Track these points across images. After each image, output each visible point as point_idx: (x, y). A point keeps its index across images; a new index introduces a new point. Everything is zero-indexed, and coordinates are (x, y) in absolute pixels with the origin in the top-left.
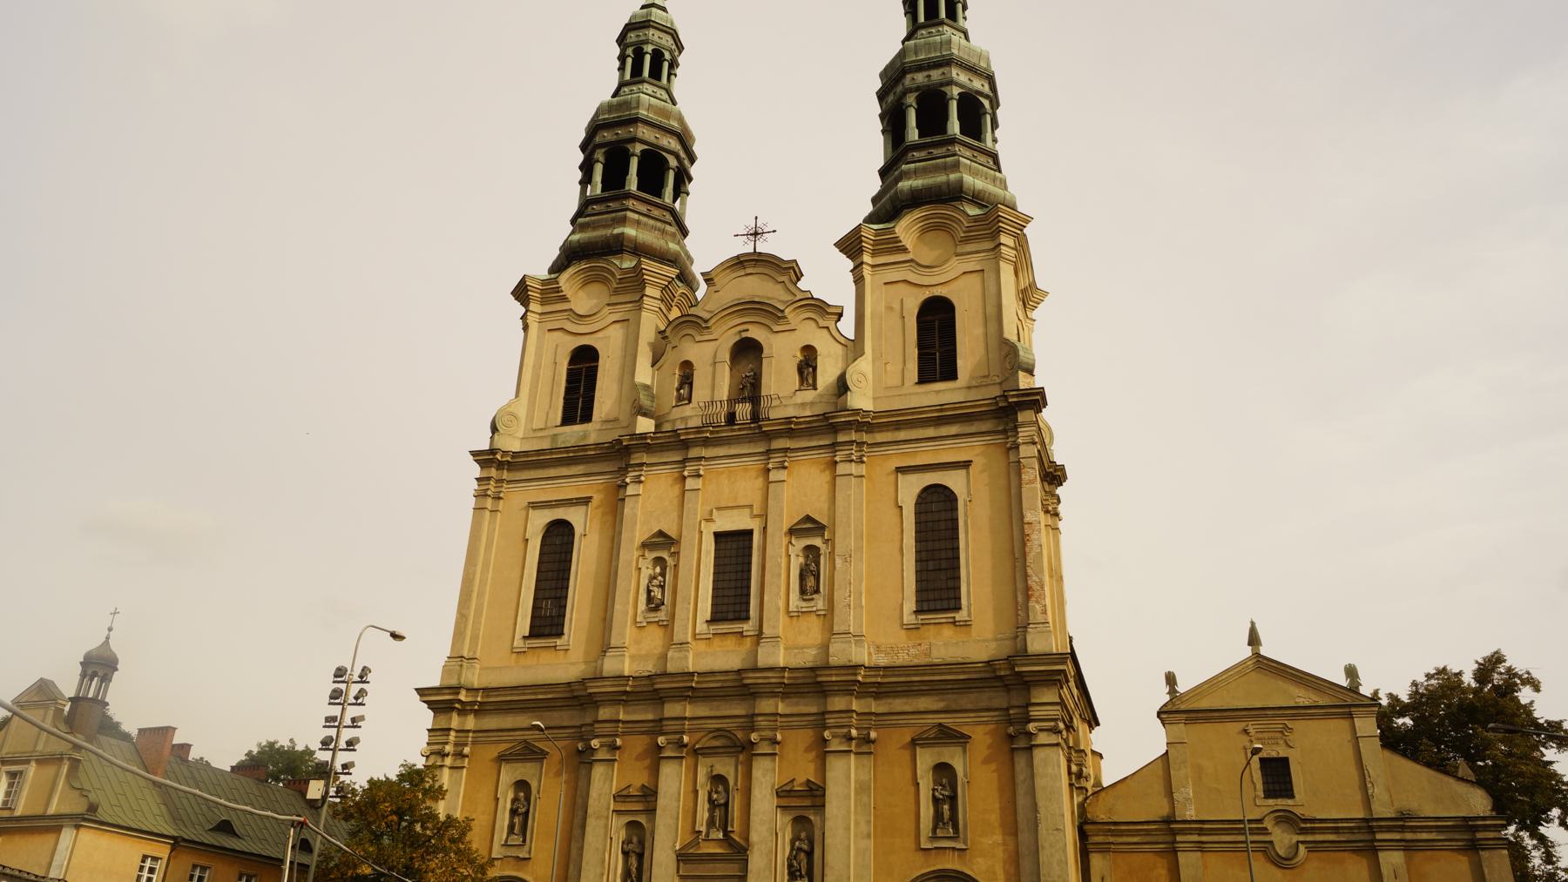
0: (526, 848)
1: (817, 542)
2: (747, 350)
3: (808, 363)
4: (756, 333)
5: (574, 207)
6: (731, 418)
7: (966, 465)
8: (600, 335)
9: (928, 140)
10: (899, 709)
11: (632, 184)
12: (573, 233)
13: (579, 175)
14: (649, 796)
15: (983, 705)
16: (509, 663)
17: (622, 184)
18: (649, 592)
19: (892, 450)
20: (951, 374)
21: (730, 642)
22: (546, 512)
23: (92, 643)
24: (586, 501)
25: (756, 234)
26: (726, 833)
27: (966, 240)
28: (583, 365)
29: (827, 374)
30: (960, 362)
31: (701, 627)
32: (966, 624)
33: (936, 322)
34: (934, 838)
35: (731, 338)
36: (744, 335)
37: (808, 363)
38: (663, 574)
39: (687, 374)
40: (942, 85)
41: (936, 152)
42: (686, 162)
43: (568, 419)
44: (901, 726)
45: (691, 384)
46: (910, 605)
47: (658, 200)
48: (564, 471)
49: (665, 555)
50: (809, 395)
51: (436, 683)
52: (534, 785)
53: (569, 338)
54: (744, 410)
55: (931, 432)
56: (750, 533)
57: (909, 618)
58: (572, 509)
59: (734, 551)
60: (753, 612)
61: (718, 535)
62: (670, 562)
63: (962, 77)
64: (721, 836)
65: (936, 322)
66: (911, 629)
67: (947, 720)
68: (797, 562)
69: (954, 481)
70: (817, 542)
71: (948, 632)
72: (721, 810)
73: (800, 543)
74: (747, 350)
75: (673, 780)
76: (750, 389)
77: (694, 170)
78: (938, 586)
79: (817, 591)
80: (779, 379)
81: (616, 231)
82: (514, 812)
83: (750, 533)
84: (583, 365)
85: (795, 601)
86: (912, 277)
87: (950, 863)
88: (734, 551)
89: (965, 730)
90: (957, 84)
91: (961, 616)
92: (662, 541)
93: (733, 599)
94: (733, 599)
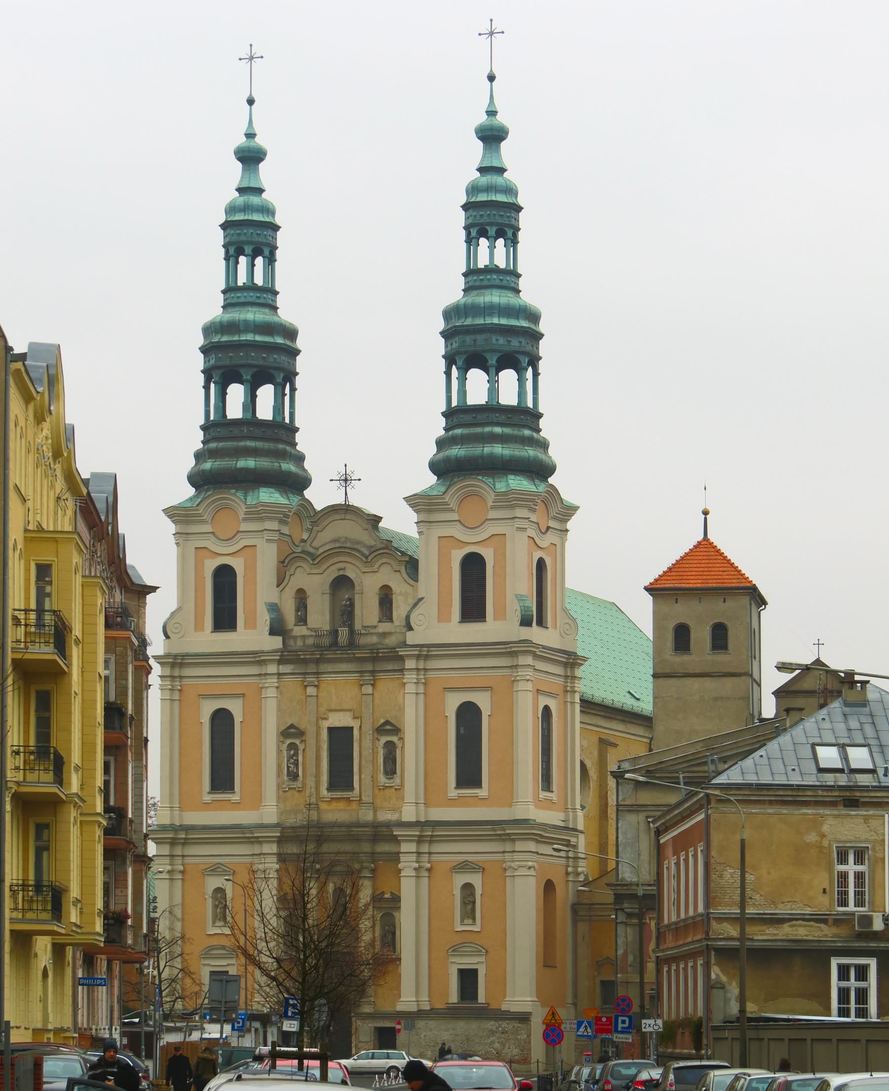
18: (288, 767)
21: (342, 805)
25: (346, 480)
28: (224, 579)
31: (324, 792)
35: (332, 574)
38: (296, 754)
39: (301, 598)
45: (306, 608)
49: (297, 742)
54: (343, 632)
59: (341, 740)
61: (330, 729)
62: (301, 747)
70: (394, 739)
74: (342, 583)
76: (345, 613)
79: (395, 773)
80: (367, 612)
82: (216, 907)
84: (224, 579)
85: (382, 779)
88: (341, 740)
90: (494, 351)
93: (341, 776)
94: (341, 776)
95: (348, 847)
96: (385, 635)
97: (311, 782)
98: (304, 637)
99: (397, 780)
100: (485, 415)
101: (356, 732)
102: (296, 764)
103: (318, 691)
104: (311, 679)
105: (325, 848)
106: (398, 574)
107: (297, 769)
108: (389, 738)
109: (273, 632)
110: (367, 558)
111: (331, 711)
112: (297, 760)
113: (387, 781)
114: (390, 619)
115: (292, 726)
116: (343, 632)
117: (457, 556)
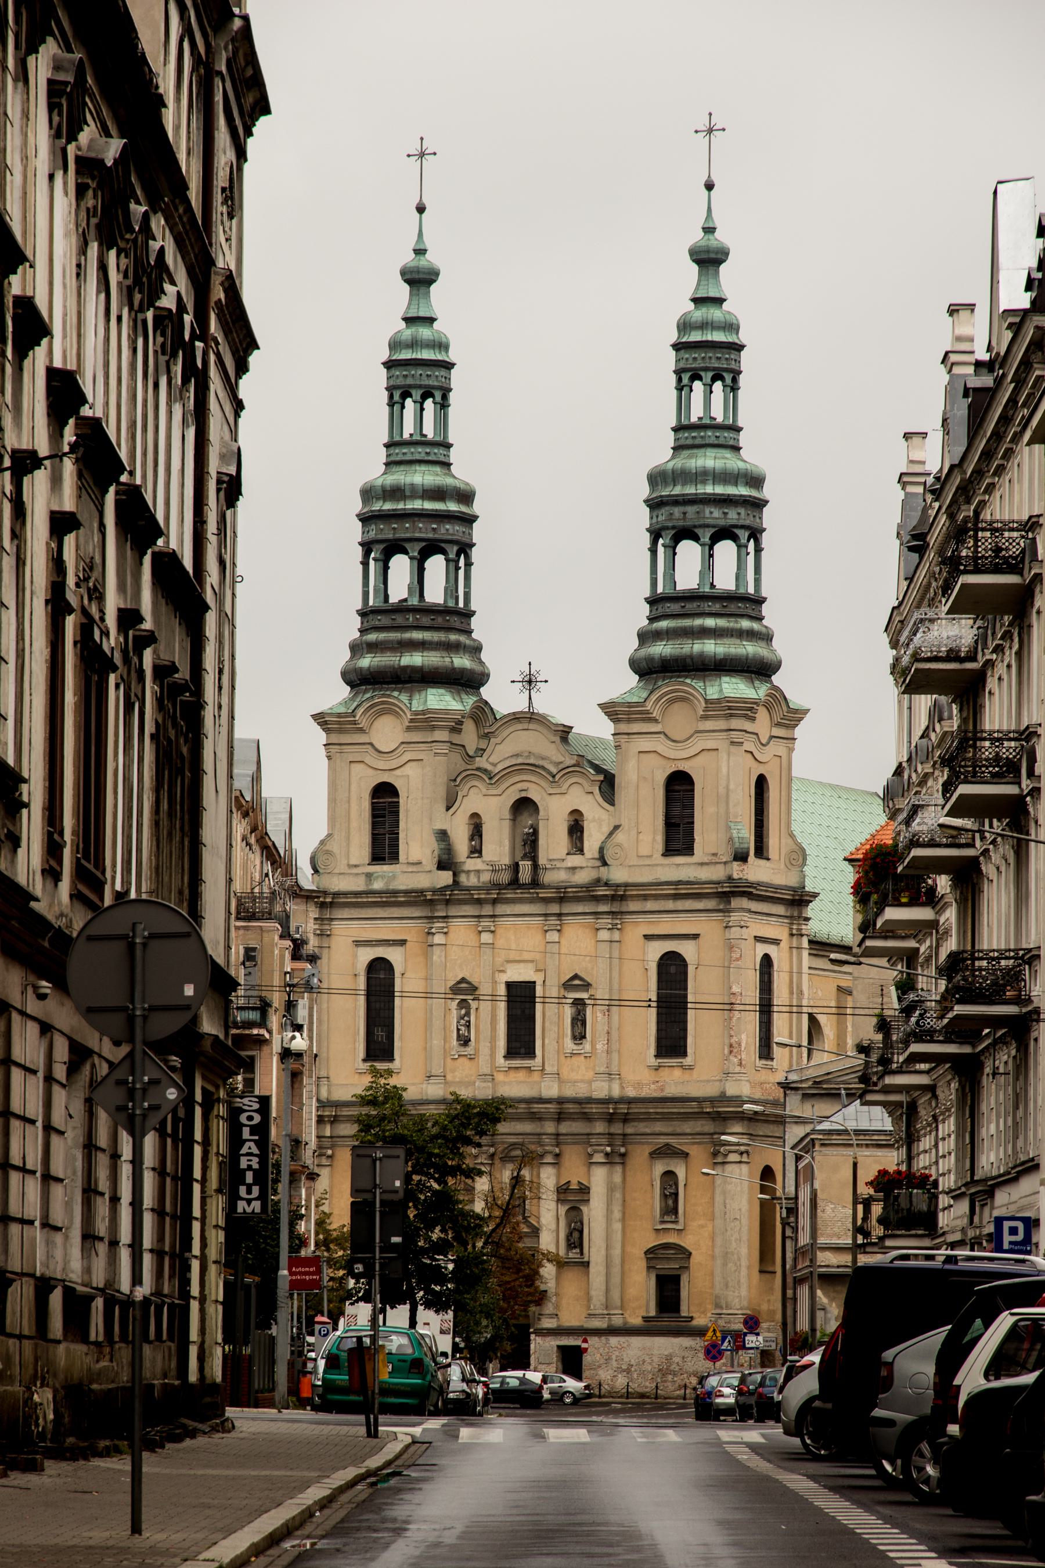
1: (584, 995)
3: (576, 829)
4: (534, 795)
8: (398, 772)
15: (698, 1130)
18: (458, 1030)
19: (641, 918)
20: (688, 849)
21: (521, 1075)
22: (368, 949)
24: (402, 943)
29: (592, 841)
31: (501, 1061)
32: (690, 1068)
36: (524, 794)
37: (576, 829)
38: (468, 1014)
43: (377, 857)
44: (643, 1144)
45: (481, 836)
46: (652, 1051)
53: (371, 772)
58: (390, 949)
59: (521, 999)
67: (673, 1141)
71: (677, 1073)
86: (660, 748)
88: (521, 999)
89: (685, 1149)
91: (688, 1061)
93: (521, 1041)
94: (521, 1041)
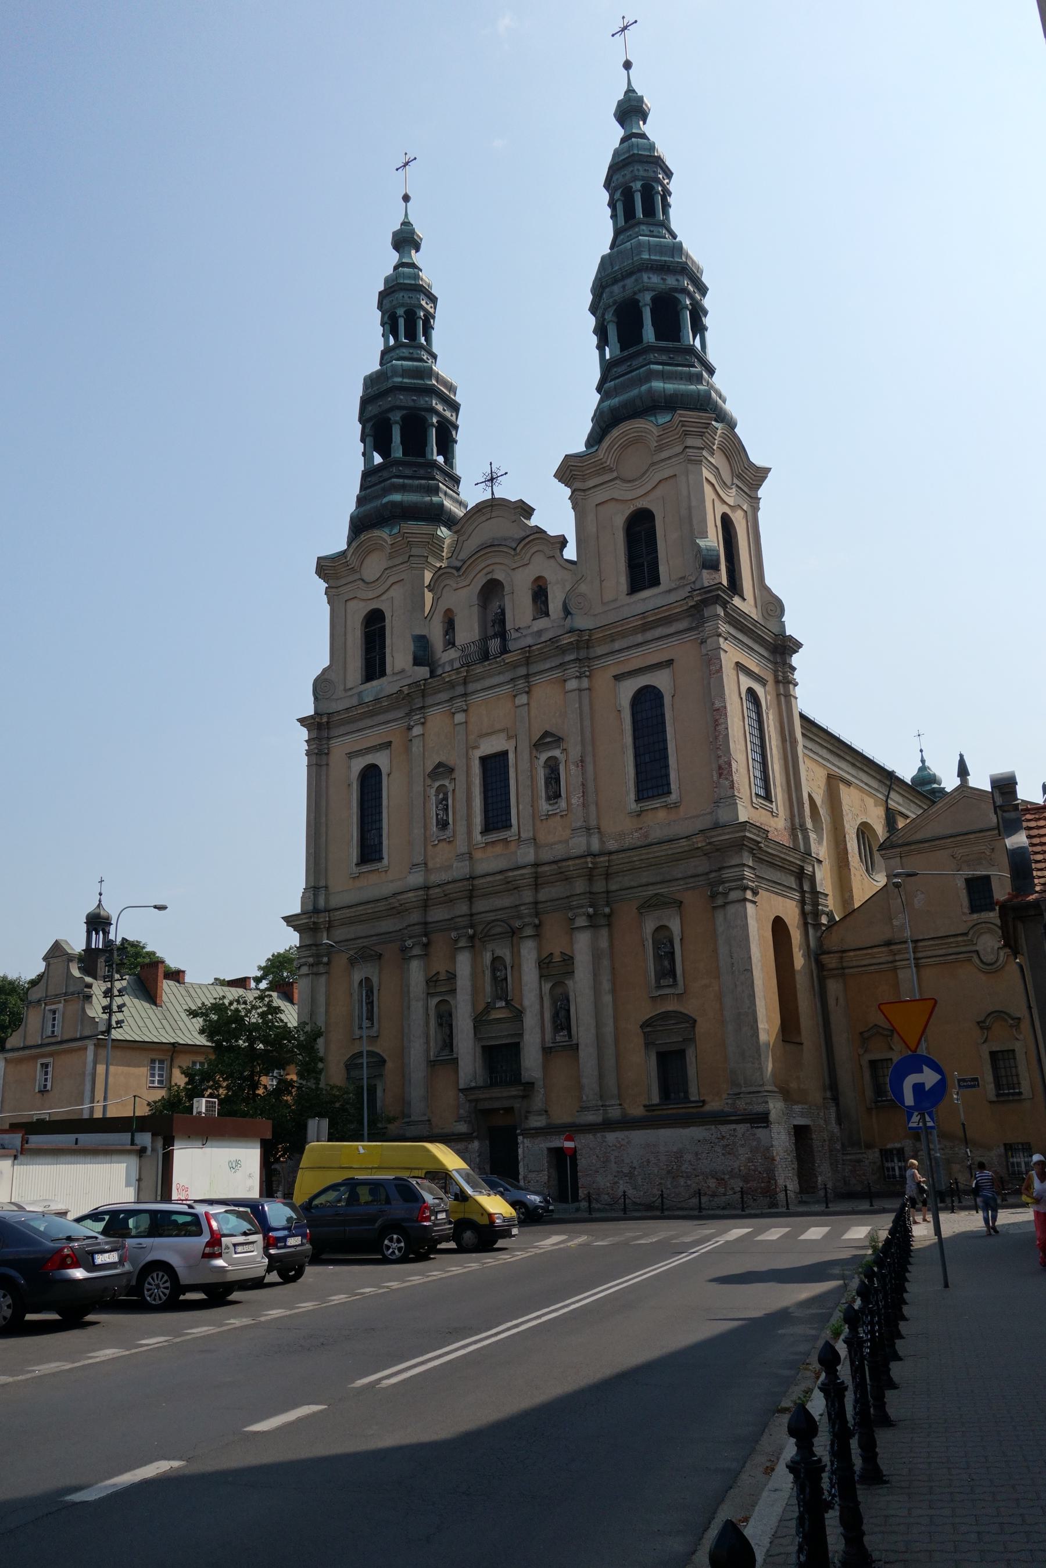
0: (375, 1029)
1: (557, 753)
2: (492, 589)
3: (540, 594)
4: (499, 576)
5: (596, 375)
6: (485, 656)
7: (670, 663)
8: (384, 597)
9: (632, 350)
10: (644, 881)
11: (649, 334)
12: (601, 401)
13: (594, 340)
14: (452, 977)
16: (349, 887)
17: (639, 339)
18: (437, 815)
19: (610, 660)
21: (498, 849)
23: (91, 907)
25: (492, 479)
26: (507, 1002)
27: (660, 448)
28: (374, 627)
30: (663, 569)
31: (478, 838)
32: (676, 806)
33: (640, 530)
34: (659, 987)
36: (489, 577)
37: (540, 594)
38: (446, 799)
40: (635, 293)
41: (635, 363)
42: (698, 296)
45: (454, 629)
47: (421, 460)
48: (369, 722)
50: (542, 623)
51: (297, 910)
52: (375, 980)
53: (362, 604)
54: (494, 645)
55: (639, 638)
56: (505, 753)
57: (633, 806)
59: (495, 768)
60: (514, 821)
61: (484, 760)
62: (450, 788)
63: (654, 279)
64: (503, 1004)
65: (640, 530)
66: (639, 814)
68: (541, 774)
69: (661, 680)
70: (557, 753)
71: (662, 814)
72: (500, 983)
73: (543, 757)
74: (492, 589)
75: (463, 964)
77: (707, 302)
78: (652, 777)
79: (560, 796)
80: (519, 610)
81: (385, 500)
83: (505, 753)
84: (374, 627)
85: (544, 806)
87: (671, 1006)
88: (495, 768)
91: (674, 797)
92: (443, 770)
95: (506, 901)
96: (540, 633)
97: (461, 829)
98: (451, 662)
99: (563, 804)
100: (641, 359)
101: (511, 756)
102: (446, 809)
103: (467, 716)
104: (459, 703)
105: (481, 905)
106: (552, 561)
107: (447, 815)
108: (550, 754)
109: (417, 662)
110: (515, 549)
111: (481, 736)
112: (447, 805)
113: (550, 808)
114: (547, 615)
115: (440, 765)
116: (494, 645)
117: (620, 521)
